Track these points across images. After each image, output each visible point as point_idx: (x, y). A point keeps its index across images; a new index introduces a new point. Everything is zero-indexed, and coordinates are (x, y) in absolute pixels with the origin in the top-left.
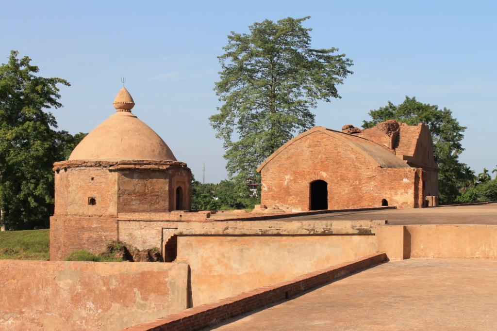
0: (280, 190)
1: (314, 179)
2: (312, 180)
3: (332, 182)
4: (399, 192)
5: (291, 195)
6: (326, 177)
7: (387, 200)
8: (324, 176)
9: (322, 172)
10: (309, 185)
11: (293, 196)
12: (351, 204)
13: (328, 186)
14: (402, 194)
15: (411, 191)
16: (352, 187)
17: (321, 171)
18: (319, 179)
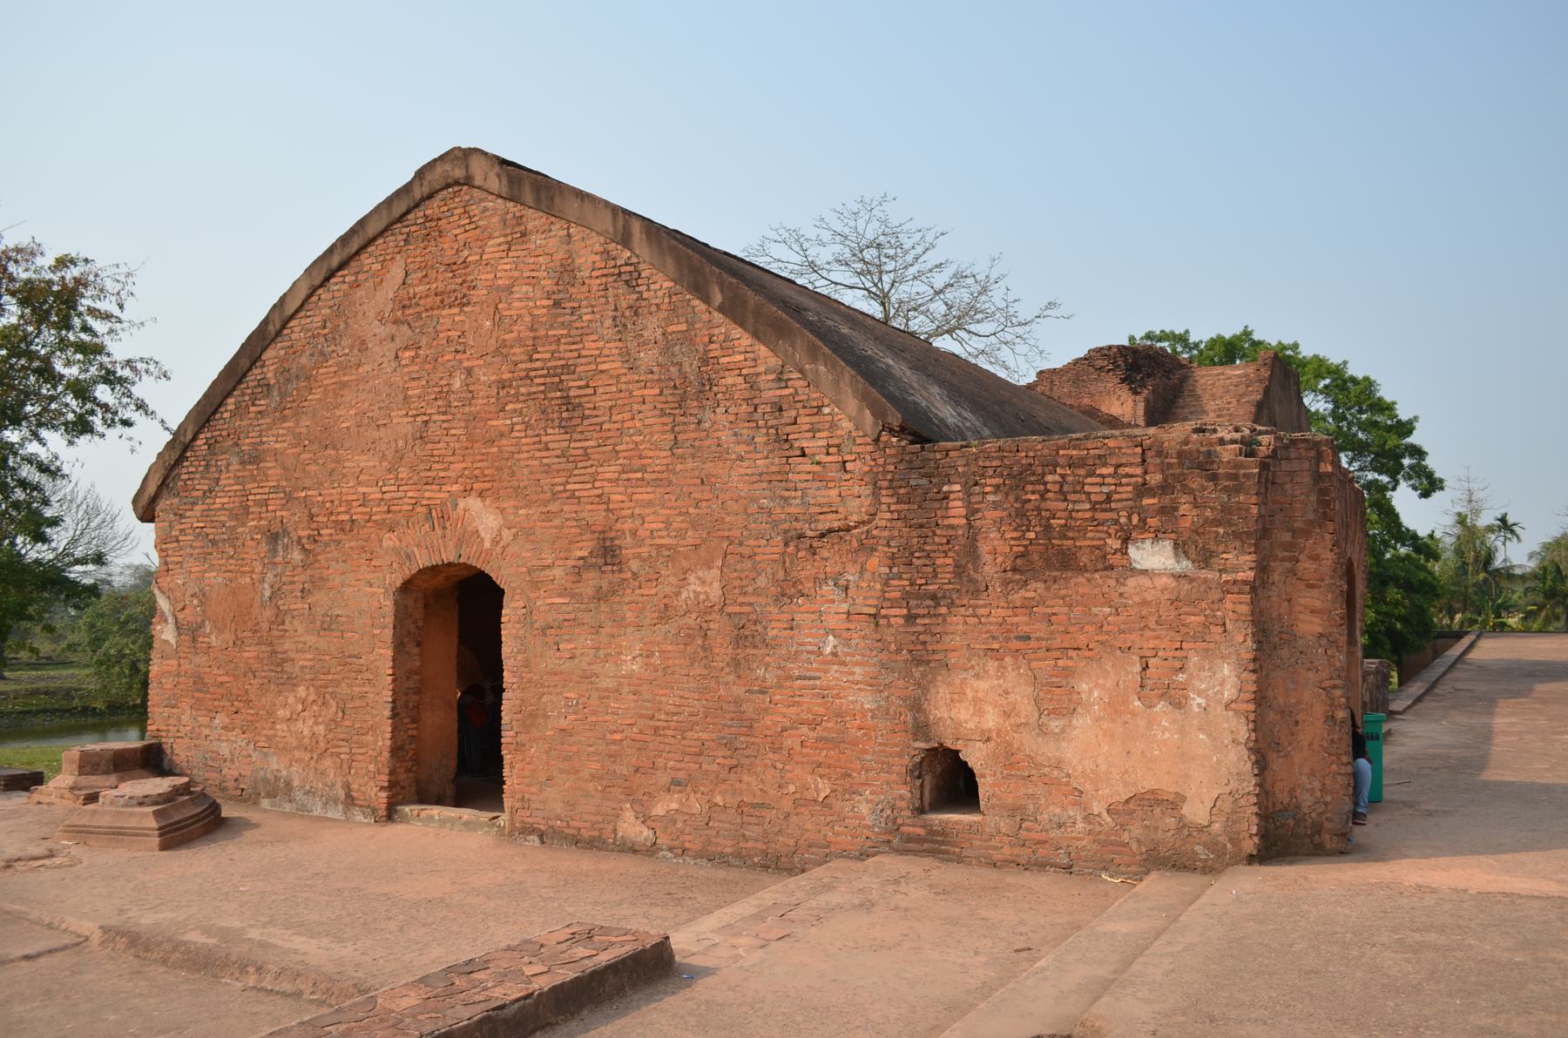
0: (238, 642)
1: (423, 560)
2: (410, 570)
3: (535, 585)
4: (1092, 688)
5: (291, 683)
6: (495, 542)
7: (974, 756)
8: (486, 531)
9: (473, 503)
10: (388, 605)
11: (301, 691)
12: (664, 779)
13: (510, 612)
14: (1116, 707)
15: (1220, 681)
16: (671, 627)
17: (467, 491)
18: (449, 556)
